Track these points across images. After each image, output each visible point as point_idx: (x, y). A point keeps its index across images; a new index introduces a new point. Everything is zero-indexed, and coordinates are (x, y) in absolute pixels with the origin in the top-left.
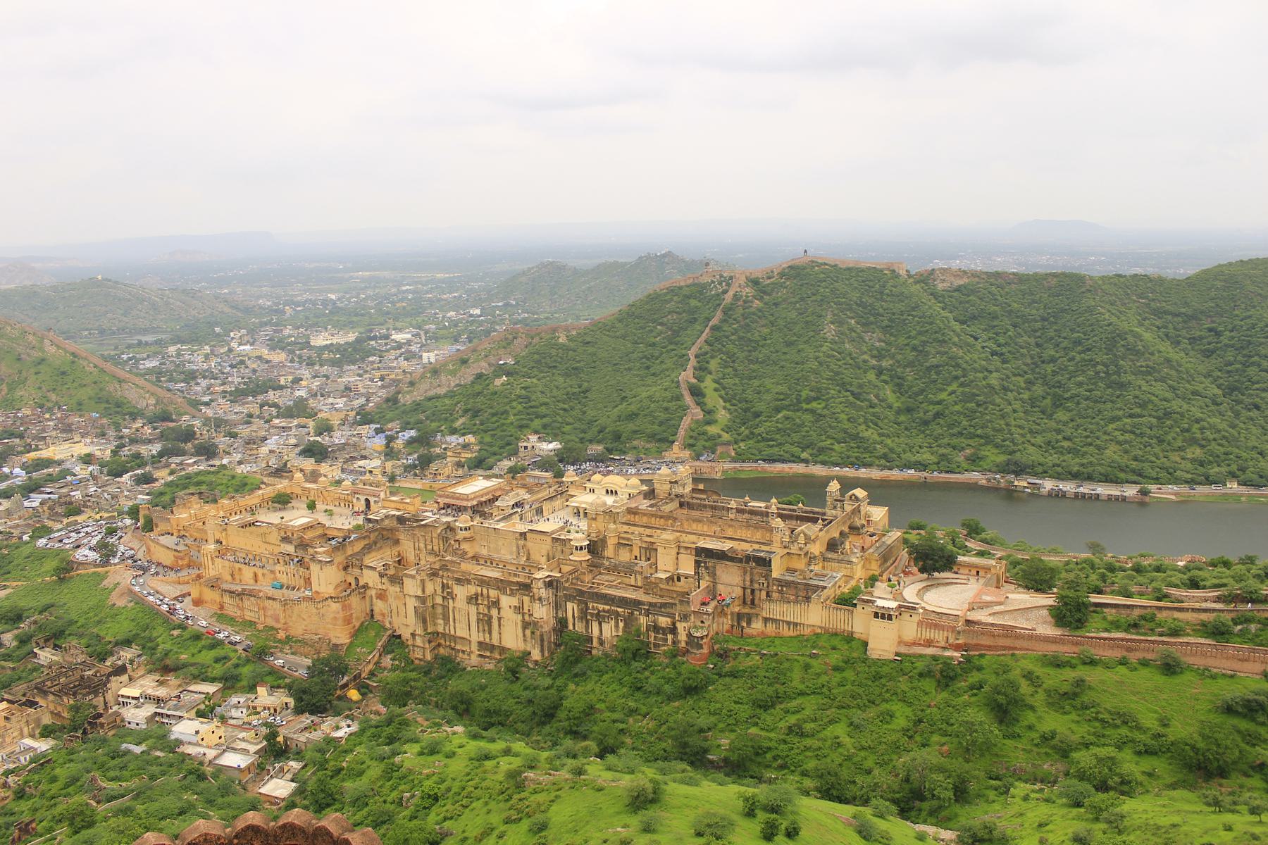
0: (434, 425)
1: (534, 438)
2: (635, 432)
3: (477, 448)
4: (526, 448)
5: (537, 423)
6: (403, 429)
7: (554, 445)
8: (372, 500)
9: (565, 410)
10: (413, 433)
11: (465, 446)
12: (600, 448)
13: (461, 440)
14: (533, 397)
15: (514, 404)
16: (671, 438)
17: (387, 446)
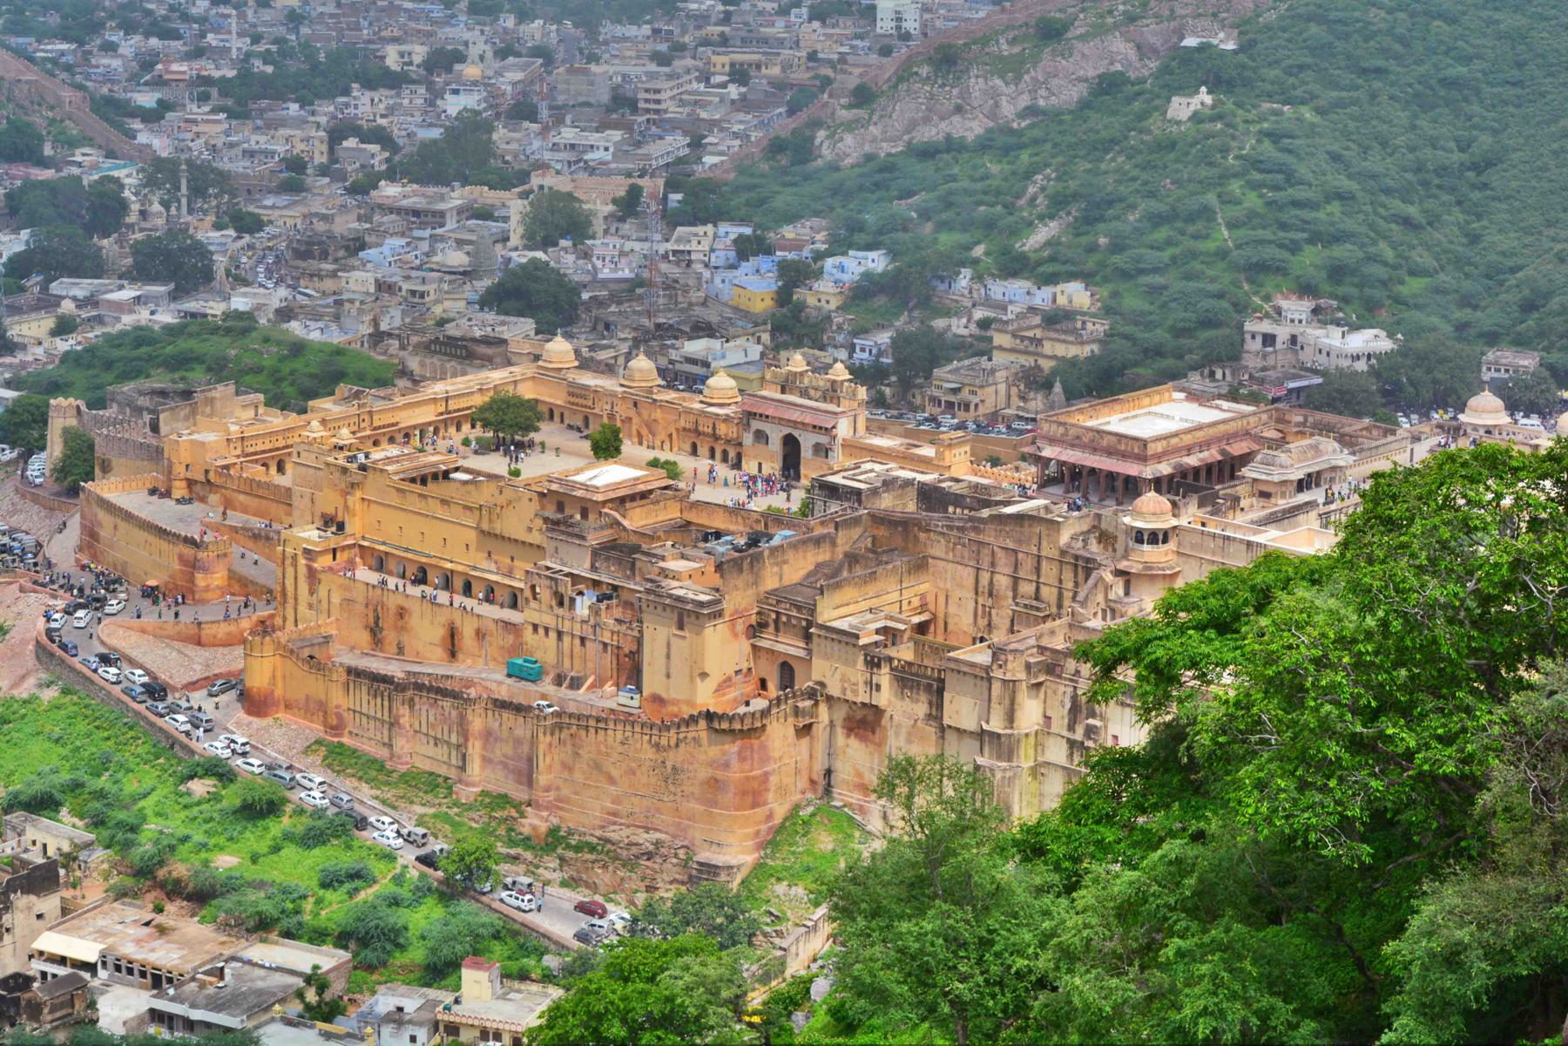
0: (947, 240)
1: (1297, 308)
3: (1099, 328)
4: (1269, 339)
5: (1310, 259)
6: (839, 246)
7: (1369, 341)
8: (807, 441)
9: (1407, 222)
10: (877, 262)
11: (1056, 319)
12: (1528, 361)
13: (1043, 297)
14: (1303, 170)
15: (1235, 186)
17: (783, 297)
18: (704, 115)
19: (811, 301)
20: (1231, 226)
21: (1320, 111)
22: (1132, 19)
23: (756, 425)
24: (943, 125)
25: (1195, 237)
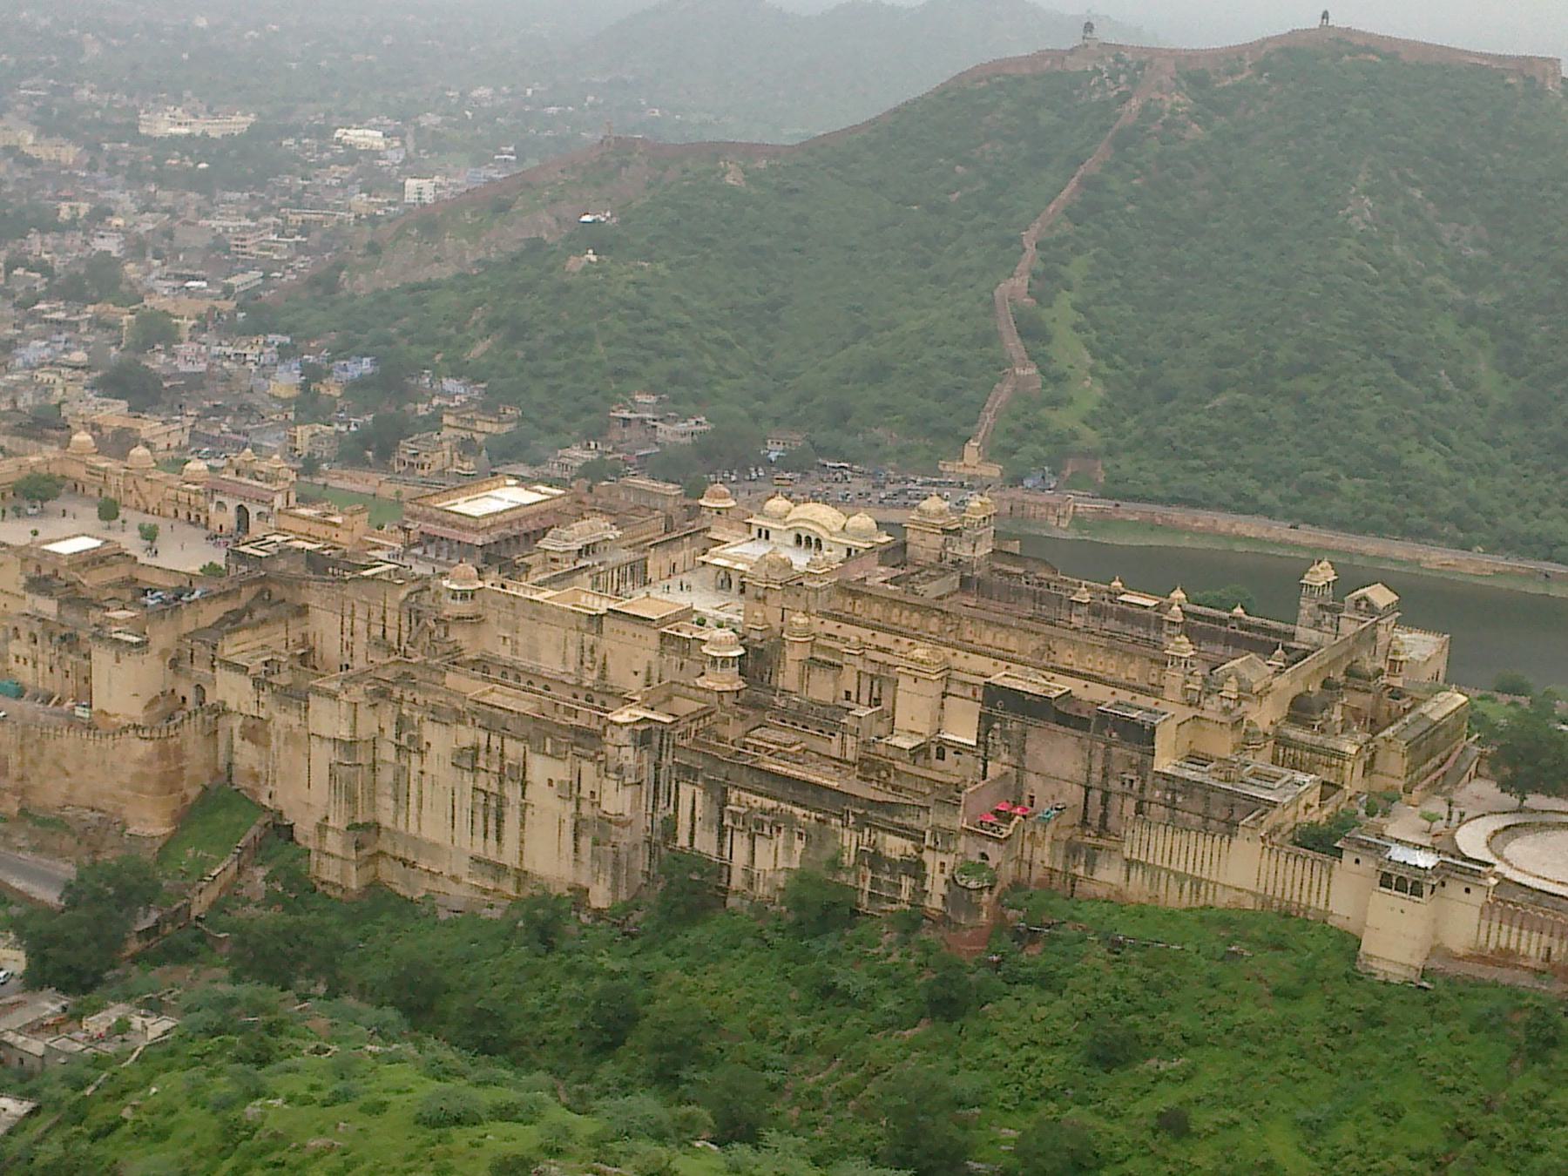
0: (417, 351)
2: (882, 408)
4: (626, 421)
9: (722, 343)
10: (366, 366)
16: (964, 431)
17: (305, 387)
18: (276, 257)
19: (323, 390)
20: (607, 344)
21: (670, 267)
22: (553, 201)
23: (218, 498)
24: (426, 270)
25: (582, 352)
